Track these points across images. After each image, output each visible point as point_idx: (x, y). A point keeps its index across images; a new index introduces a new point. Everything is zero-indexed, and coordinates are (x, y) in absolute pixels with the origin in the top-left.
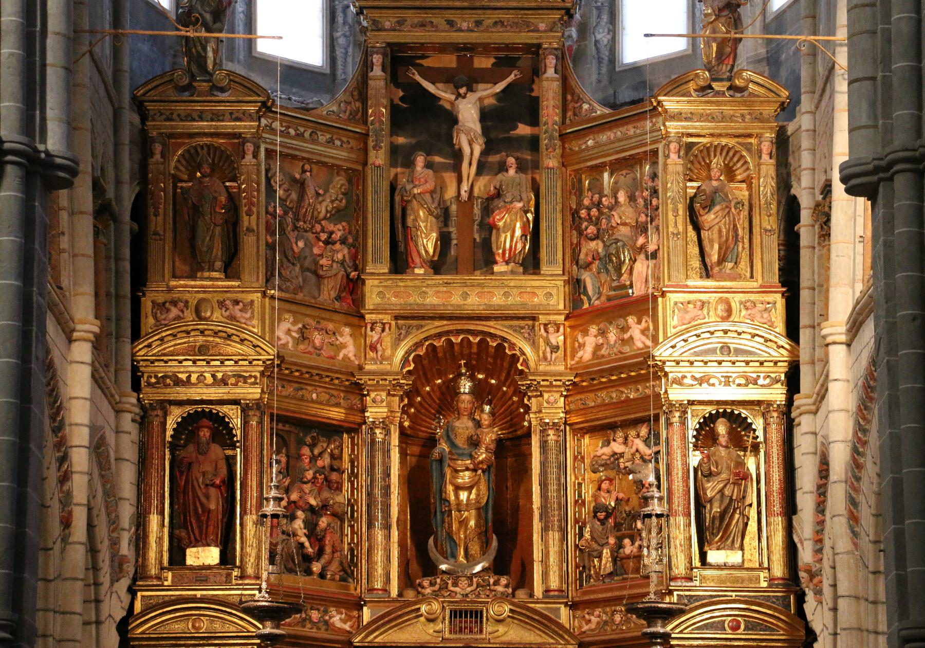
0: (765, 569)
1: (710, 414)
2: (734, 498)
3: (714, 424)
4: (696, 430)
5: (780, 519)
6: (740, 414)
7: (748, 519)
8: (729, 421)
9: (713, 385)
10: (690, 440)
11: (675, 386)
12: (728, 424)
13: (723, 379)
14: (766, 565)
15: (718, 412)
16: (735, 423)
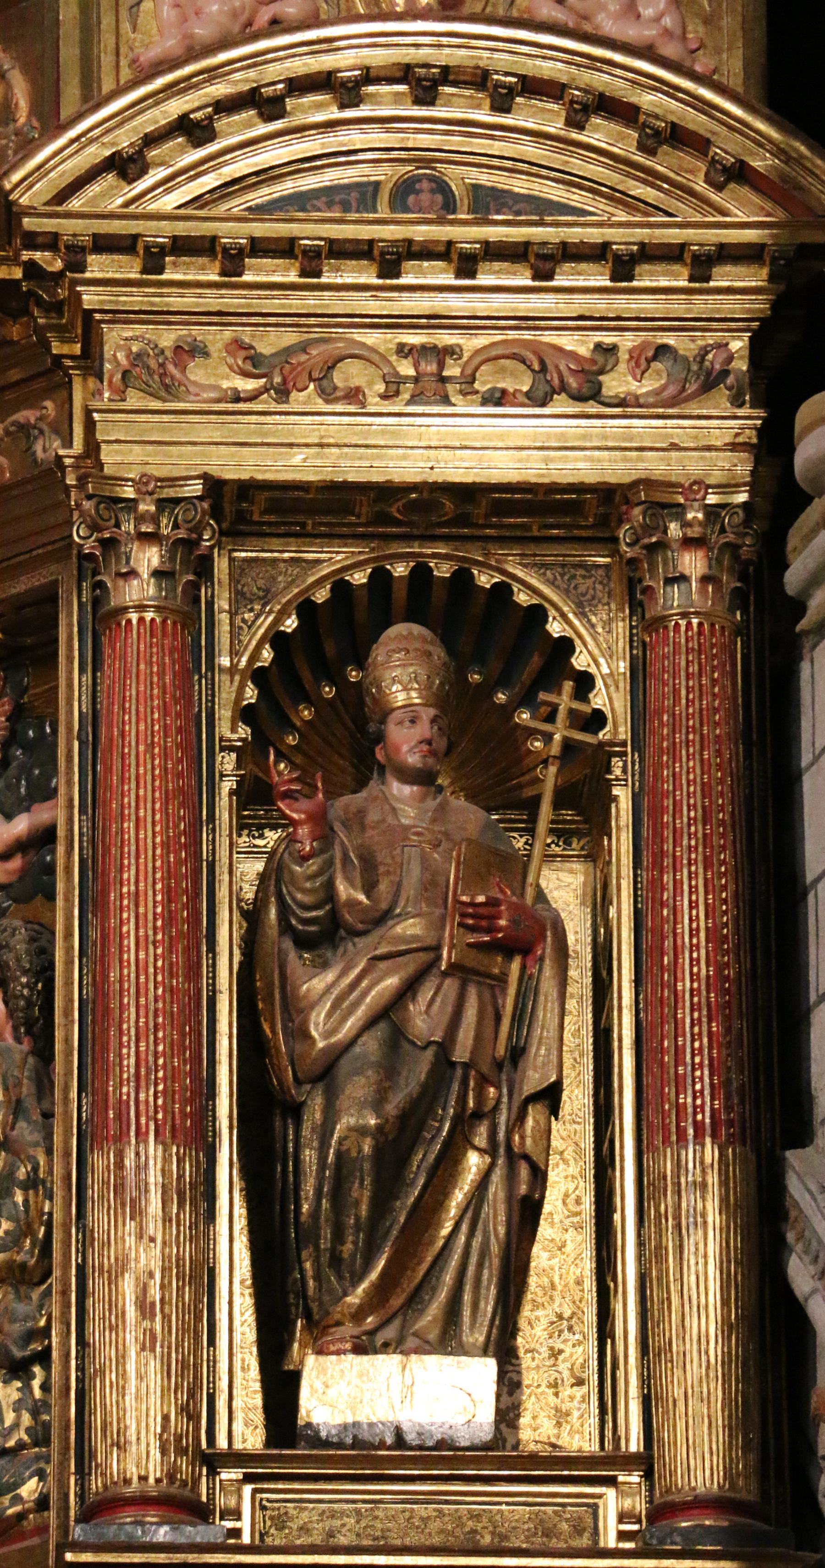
0: (628, 1462)
1: (341, 588)
2: (461, 1053)
3: (361, 663)
4: (259, 676)
5: (710, 1152)
6: (502, 591)
7: (539, 1176)
8: (447, 640)
9: (354, 395)
10: (223, 729)
11: (134, 399)
12: (439, 653)
13: (406, 369)
14: (635, 1445)
15: (380, 577)
16: (479, 658)
